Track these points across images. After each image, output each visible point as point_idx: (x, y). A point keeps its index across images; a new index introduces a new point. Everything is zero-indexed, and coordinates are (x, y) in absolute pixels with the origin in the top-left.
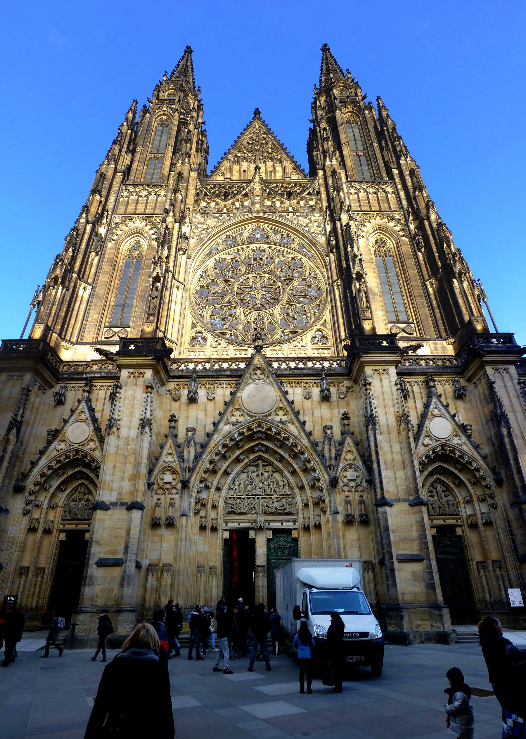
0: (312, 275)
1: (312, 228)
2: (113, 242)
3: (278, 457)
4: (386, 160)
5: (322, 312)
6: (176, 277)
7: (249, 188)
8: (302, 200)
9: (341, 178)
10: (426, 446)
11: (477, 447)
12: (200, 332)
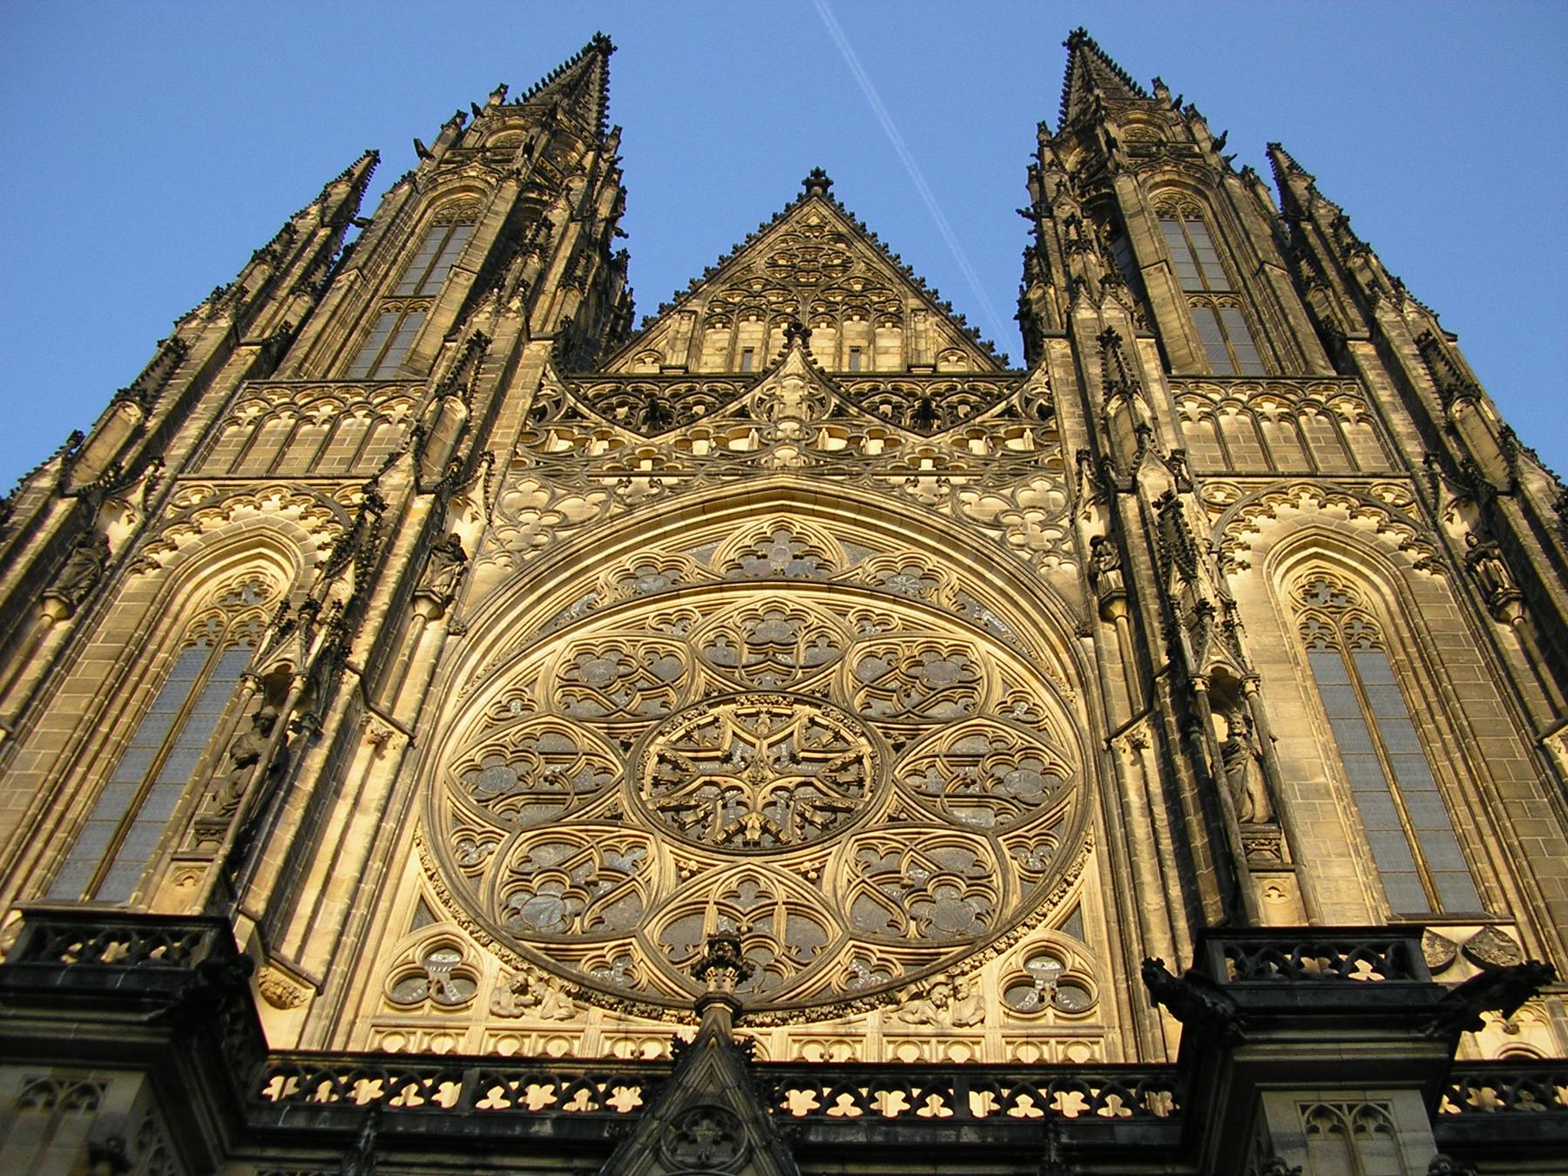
1: (1021, 528)
2: (151, 573)
4: (1321, 316)
7: (757, 392)
8: (977, 435)
9: (1137, 359)
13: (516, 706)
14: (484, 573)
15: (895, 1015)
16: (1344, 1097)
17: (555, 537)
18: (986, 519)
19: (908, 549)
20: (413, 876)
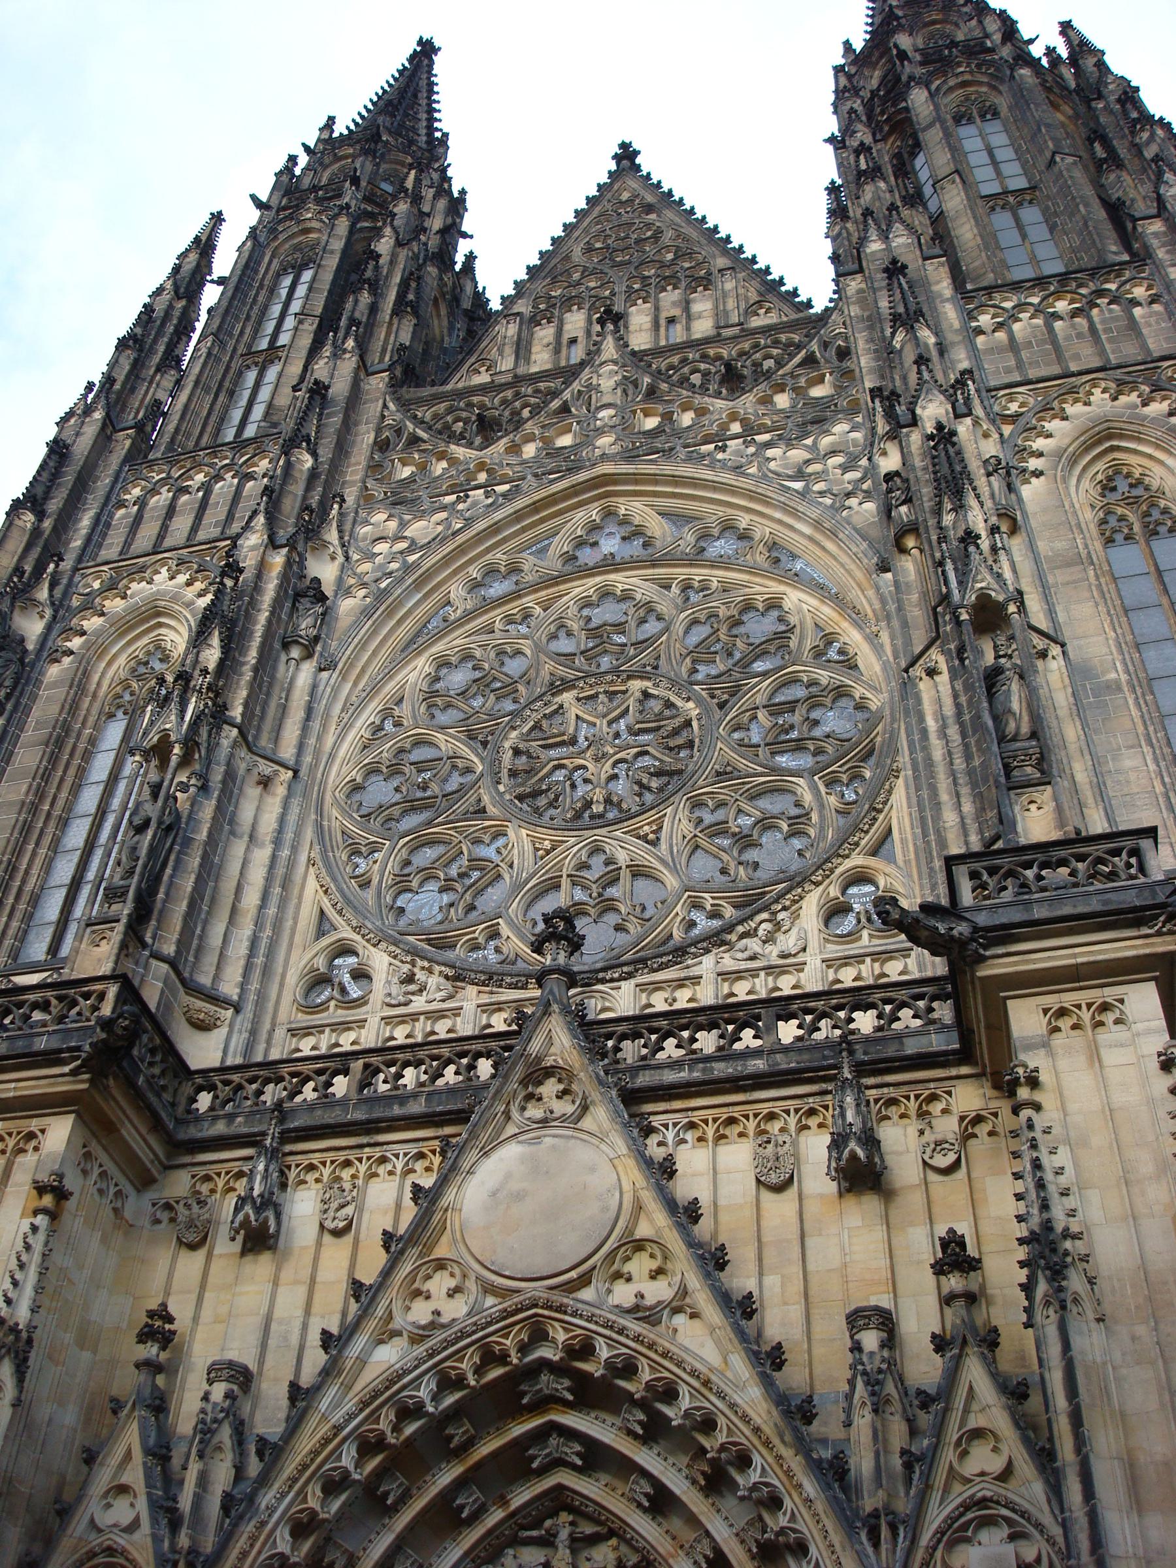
0: (832, 654)
1: (819, 476)
2: (67, 660)
6: (264, 742)
7: (576, 386)
8: (781, 388)
9: (925, 283)
12: (346, 950)
13: (389, 726)
14: (347, 607)
15: (726, 955)
17: (405, 562)
18: (790, 472)
19: (722, 512)
20: (311, 892)
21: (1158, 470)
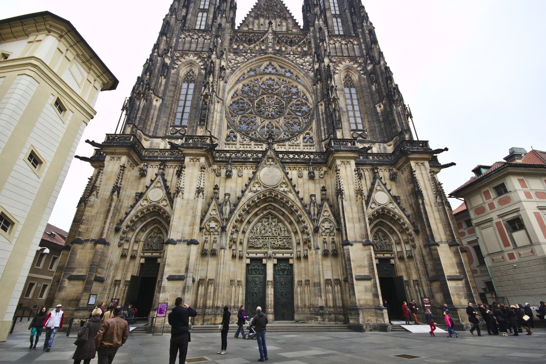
0: (304, 97)
1: (305, 66)
2: (175, 70)
3: (281, 213)
4: (354, 21)
5: (310, 122)
8: (299, 47)
10: (372, 209)
11: (403, 210)
12: (232, 132)
14: (228, 71)
16: (345, 160)
21: (353, 76)
